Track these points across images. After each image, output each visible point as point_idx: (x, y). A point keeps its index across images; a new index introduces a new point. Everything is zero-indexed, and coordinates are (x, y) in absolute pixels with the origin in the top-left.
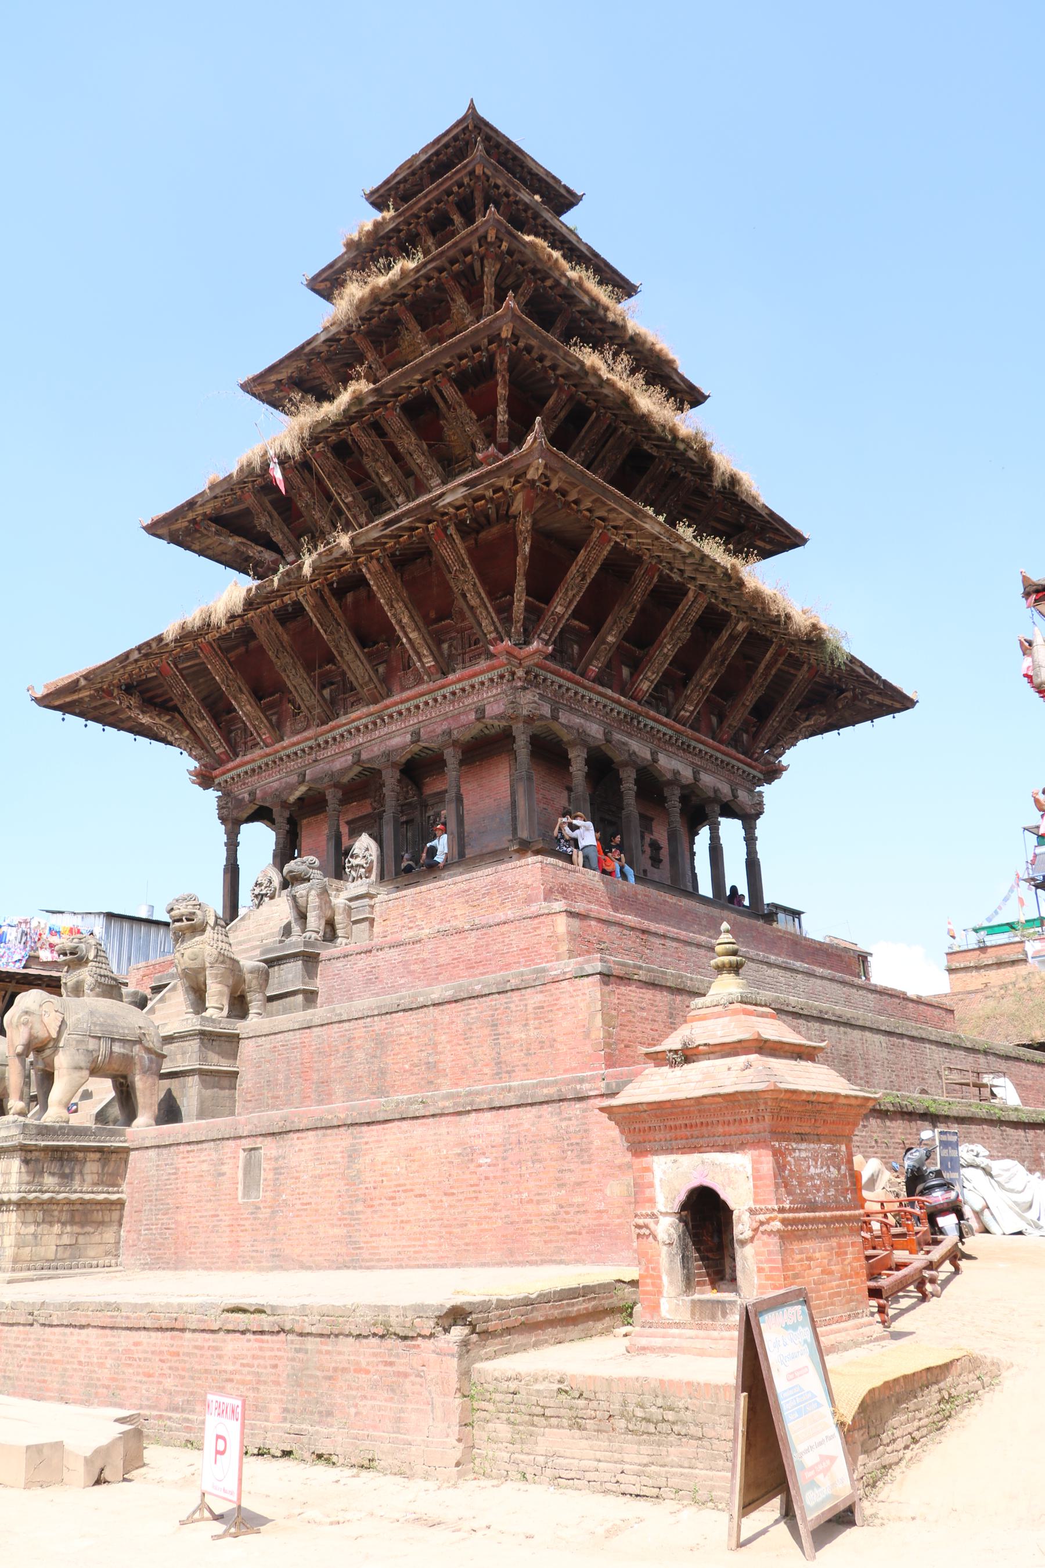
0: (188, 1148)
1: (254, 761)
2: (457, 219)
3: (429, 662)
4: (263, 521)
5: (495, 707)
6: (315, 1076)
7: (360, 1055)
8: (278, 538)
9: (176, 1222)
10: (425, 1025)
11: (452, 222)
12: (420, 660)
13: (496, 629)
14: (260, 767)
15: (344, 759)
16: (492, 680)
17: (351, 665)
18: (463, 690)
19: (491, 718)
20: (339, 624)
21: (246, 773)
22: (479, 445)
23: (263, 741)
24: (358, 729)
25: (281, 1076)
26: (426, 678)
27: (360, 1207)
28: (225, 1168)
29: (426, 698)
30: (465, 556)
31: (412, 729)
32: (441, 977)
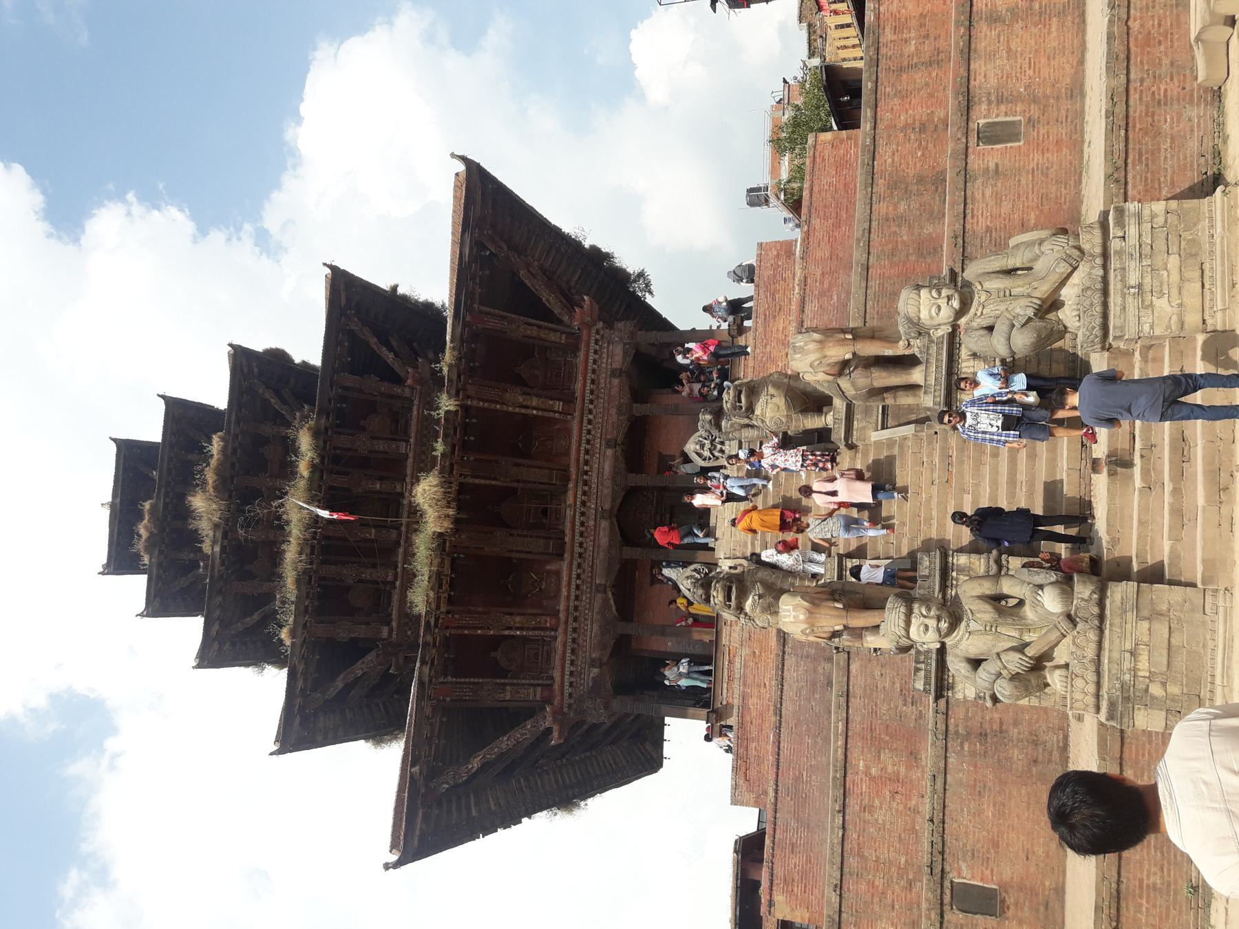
0: (969, 217)
1: (565, 645)
3: (559, 406)
5: (616, 358)
6: (912, 258)
7: (902, 206)
8: (361, 632)
12: (555, 412)
13: (562, 332)
14: (574, 640)
16: (596, 352)
18: (593, 382)
21: (572, 663)
22: (397, 390)
24: (583, 503)
28: (992, 166)
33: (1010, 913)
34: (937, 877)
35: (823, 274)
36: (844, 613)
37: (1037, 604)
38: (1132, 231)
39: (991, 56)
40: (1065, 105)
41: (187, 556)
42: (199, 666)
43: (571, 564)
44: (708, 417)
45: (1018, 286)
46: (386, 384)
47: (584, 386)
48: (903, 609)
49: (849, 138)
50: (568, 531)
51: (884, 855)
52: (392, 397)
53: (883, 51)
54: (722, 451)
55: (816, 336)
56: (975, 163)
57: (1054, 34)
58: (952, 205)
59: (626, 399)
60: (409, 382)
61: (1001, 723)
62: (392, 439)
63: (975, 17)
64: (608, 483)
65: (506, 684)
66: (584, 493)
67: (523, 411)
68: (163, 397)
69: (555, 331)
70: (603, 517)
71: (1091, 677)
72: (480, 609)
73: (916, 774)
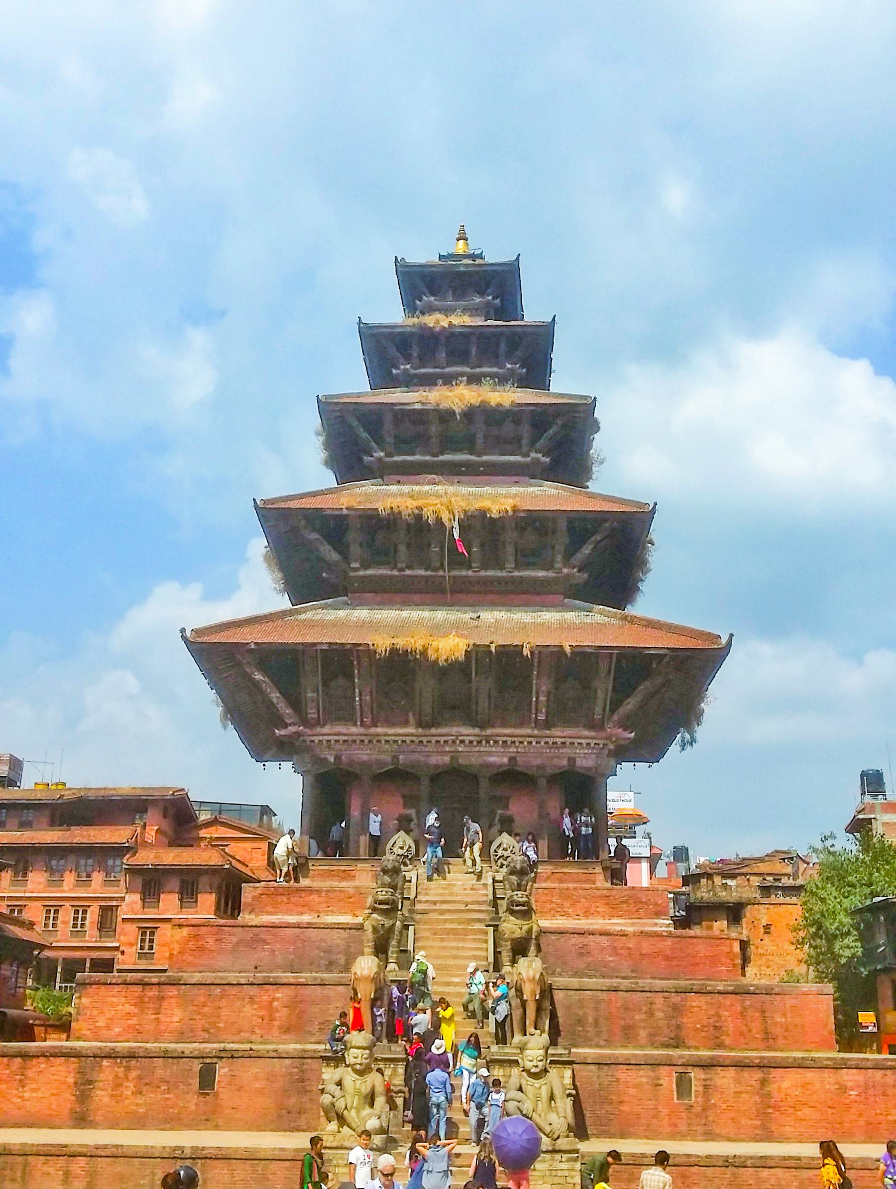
0: (627, 1067)
3: (541, 717)
6: (622, 1023)
9: (620, 1110)
10: (712, 1004)
12: (536, 714)
14: (354, 741)
15: (439, 758)
16: (589, 744)
18: (563, 743)
21: (336, 741)
23: (362, 721)
24: (462, 742)
25: (590, 1019)
26: (533, 725)
27: (770, 1111)
28: (661, 1082)
31: (510, 755)
32: (644, 962)
33: (201, 1098)
34: (218, 1054)
35: (629, 949)
36: (368, 999)
37: (370, 1116)
38: (564, 1166)
39: (737, 1081)
40: (700, 1129)
43: (413, 735)
45: (542, 1105)
48: (365, 1045)
49: (734, 965)
51: (224, 1012)
52: (553, 548)
53: (778, 998)
54: (501, 867)
55: (537, 977)
56: (663, 1071)
57: (749, 1122)
58: (635, 1055)
59: (549, 771)
60: (565, 570)
61: (310, 1091)
63: (766, 1070)
64: (480, 761)
66: (471, 742)
67: (534, 691)
70: (452, 758)
71: (334, 1144)
73: (275, 1031)
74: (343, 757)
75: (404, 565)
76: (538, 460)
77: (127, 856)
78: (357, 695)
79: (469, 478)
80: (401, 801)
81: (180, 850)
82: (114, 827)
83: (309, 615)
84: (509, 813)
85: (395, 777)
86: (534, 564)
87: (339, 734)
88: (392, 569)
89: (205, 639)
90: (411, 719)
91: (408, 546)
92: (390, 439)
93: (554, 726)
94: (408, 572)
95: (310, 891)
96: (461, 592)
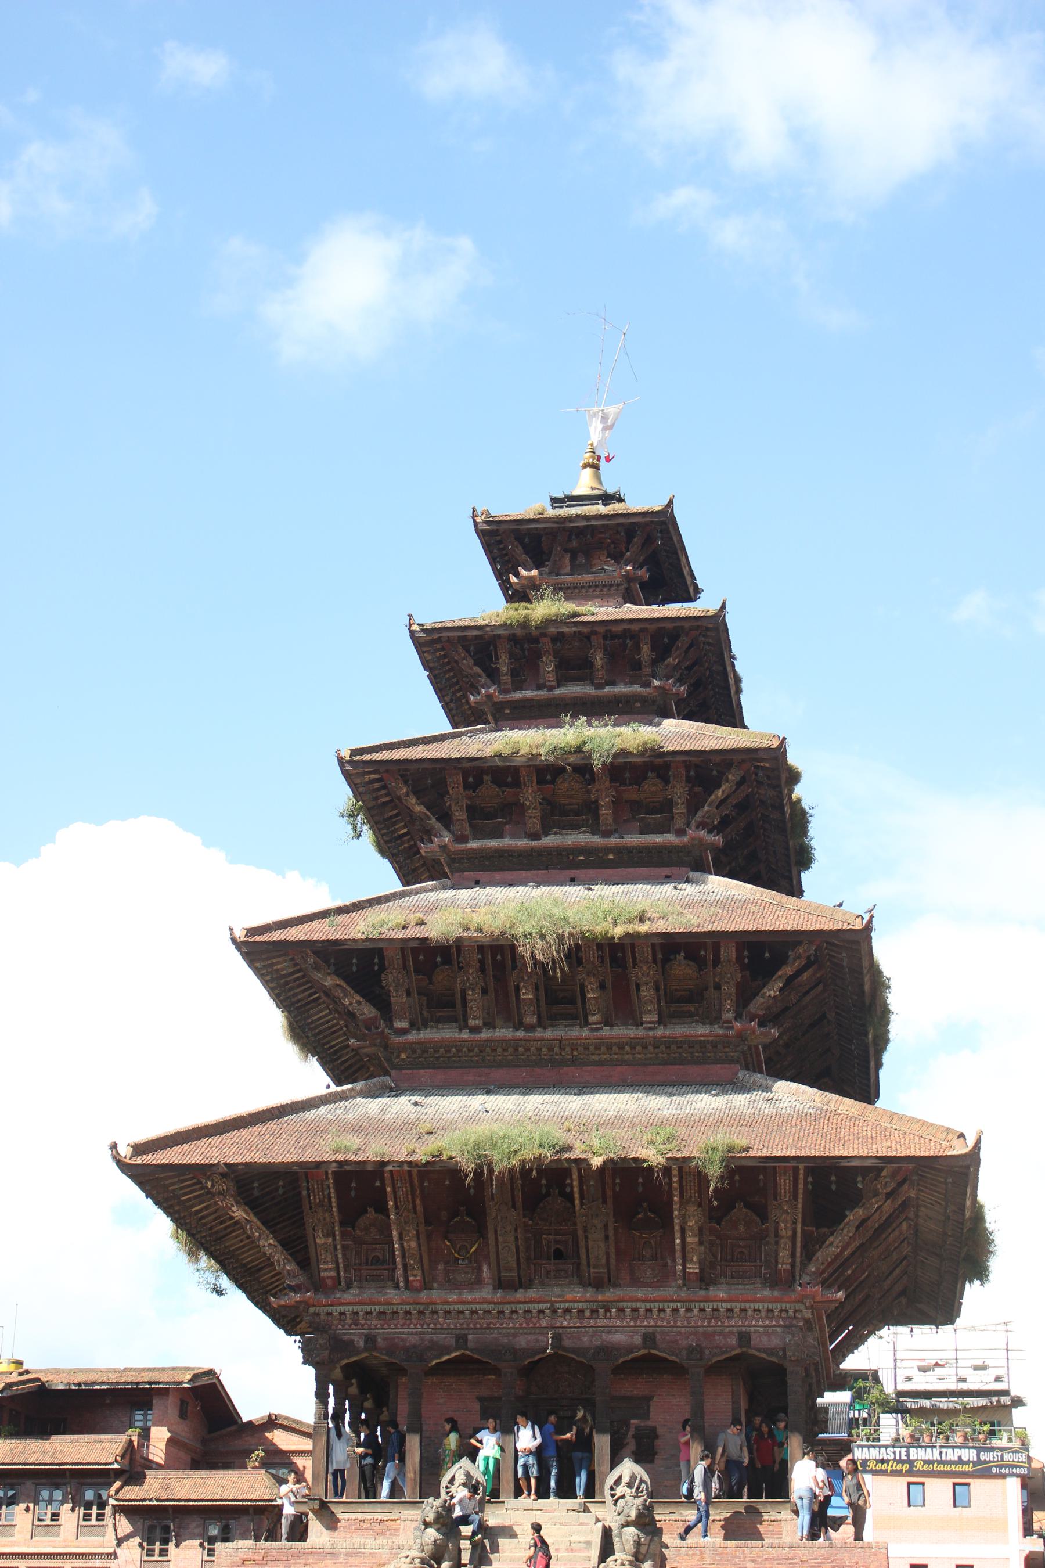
2: (645, 649)
3: (693, 1268)
4: (391, 978)
5: (765, 1339)
8: (398, 999)
11: (638, 649)
15: (531, 1338)
16: (769, 1311)
17: (590, 1243)
19: (759, 1350)
20: (605, 1202)
21: (367, 1313)
22: (728, 1004)
23: (407, 1281)
24: (567, 1311)
26: (680, 1282)
29: (679, 1305)
30: (801, 1191)
31: (643, 1330)
41: (504, 665)
42: (340, 760)
44: (633, 1514)
46: (733, 990)
47: (722, 1301)
50: (532, 1293)
60: (738, 1025)
62: (659, 1001)
65: (334, 1235)
66: (581, 1311)
67: (677, 1228)
68: (723, 606)
69: (793, 1255)
72: (418, 1202)
74: (379, 1340)
75: (478, 1022)
76: (701, 840)
77: (117, 1484)
78: (395, 1239)
79: (591, 873)
80: (477, 1406)
81: (204, 1473)
82: (93, 1437)
83: (323, 1110)
84: (650, 1423)
85: (467, 1366)
86: (691, 1015)
87: (374, 1303)
88: (460, 1030)
89: (149, 1159)
90: (486, 1273)
91: (484, 991)
92: (460, 815)
93: (714, 1282)
94: (485, 1034)
95: (319, 1553)
96: (574, 1062)
